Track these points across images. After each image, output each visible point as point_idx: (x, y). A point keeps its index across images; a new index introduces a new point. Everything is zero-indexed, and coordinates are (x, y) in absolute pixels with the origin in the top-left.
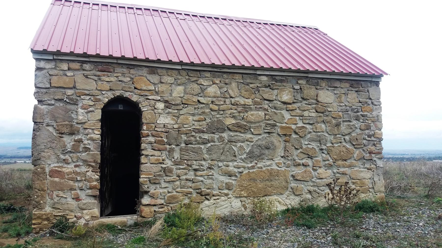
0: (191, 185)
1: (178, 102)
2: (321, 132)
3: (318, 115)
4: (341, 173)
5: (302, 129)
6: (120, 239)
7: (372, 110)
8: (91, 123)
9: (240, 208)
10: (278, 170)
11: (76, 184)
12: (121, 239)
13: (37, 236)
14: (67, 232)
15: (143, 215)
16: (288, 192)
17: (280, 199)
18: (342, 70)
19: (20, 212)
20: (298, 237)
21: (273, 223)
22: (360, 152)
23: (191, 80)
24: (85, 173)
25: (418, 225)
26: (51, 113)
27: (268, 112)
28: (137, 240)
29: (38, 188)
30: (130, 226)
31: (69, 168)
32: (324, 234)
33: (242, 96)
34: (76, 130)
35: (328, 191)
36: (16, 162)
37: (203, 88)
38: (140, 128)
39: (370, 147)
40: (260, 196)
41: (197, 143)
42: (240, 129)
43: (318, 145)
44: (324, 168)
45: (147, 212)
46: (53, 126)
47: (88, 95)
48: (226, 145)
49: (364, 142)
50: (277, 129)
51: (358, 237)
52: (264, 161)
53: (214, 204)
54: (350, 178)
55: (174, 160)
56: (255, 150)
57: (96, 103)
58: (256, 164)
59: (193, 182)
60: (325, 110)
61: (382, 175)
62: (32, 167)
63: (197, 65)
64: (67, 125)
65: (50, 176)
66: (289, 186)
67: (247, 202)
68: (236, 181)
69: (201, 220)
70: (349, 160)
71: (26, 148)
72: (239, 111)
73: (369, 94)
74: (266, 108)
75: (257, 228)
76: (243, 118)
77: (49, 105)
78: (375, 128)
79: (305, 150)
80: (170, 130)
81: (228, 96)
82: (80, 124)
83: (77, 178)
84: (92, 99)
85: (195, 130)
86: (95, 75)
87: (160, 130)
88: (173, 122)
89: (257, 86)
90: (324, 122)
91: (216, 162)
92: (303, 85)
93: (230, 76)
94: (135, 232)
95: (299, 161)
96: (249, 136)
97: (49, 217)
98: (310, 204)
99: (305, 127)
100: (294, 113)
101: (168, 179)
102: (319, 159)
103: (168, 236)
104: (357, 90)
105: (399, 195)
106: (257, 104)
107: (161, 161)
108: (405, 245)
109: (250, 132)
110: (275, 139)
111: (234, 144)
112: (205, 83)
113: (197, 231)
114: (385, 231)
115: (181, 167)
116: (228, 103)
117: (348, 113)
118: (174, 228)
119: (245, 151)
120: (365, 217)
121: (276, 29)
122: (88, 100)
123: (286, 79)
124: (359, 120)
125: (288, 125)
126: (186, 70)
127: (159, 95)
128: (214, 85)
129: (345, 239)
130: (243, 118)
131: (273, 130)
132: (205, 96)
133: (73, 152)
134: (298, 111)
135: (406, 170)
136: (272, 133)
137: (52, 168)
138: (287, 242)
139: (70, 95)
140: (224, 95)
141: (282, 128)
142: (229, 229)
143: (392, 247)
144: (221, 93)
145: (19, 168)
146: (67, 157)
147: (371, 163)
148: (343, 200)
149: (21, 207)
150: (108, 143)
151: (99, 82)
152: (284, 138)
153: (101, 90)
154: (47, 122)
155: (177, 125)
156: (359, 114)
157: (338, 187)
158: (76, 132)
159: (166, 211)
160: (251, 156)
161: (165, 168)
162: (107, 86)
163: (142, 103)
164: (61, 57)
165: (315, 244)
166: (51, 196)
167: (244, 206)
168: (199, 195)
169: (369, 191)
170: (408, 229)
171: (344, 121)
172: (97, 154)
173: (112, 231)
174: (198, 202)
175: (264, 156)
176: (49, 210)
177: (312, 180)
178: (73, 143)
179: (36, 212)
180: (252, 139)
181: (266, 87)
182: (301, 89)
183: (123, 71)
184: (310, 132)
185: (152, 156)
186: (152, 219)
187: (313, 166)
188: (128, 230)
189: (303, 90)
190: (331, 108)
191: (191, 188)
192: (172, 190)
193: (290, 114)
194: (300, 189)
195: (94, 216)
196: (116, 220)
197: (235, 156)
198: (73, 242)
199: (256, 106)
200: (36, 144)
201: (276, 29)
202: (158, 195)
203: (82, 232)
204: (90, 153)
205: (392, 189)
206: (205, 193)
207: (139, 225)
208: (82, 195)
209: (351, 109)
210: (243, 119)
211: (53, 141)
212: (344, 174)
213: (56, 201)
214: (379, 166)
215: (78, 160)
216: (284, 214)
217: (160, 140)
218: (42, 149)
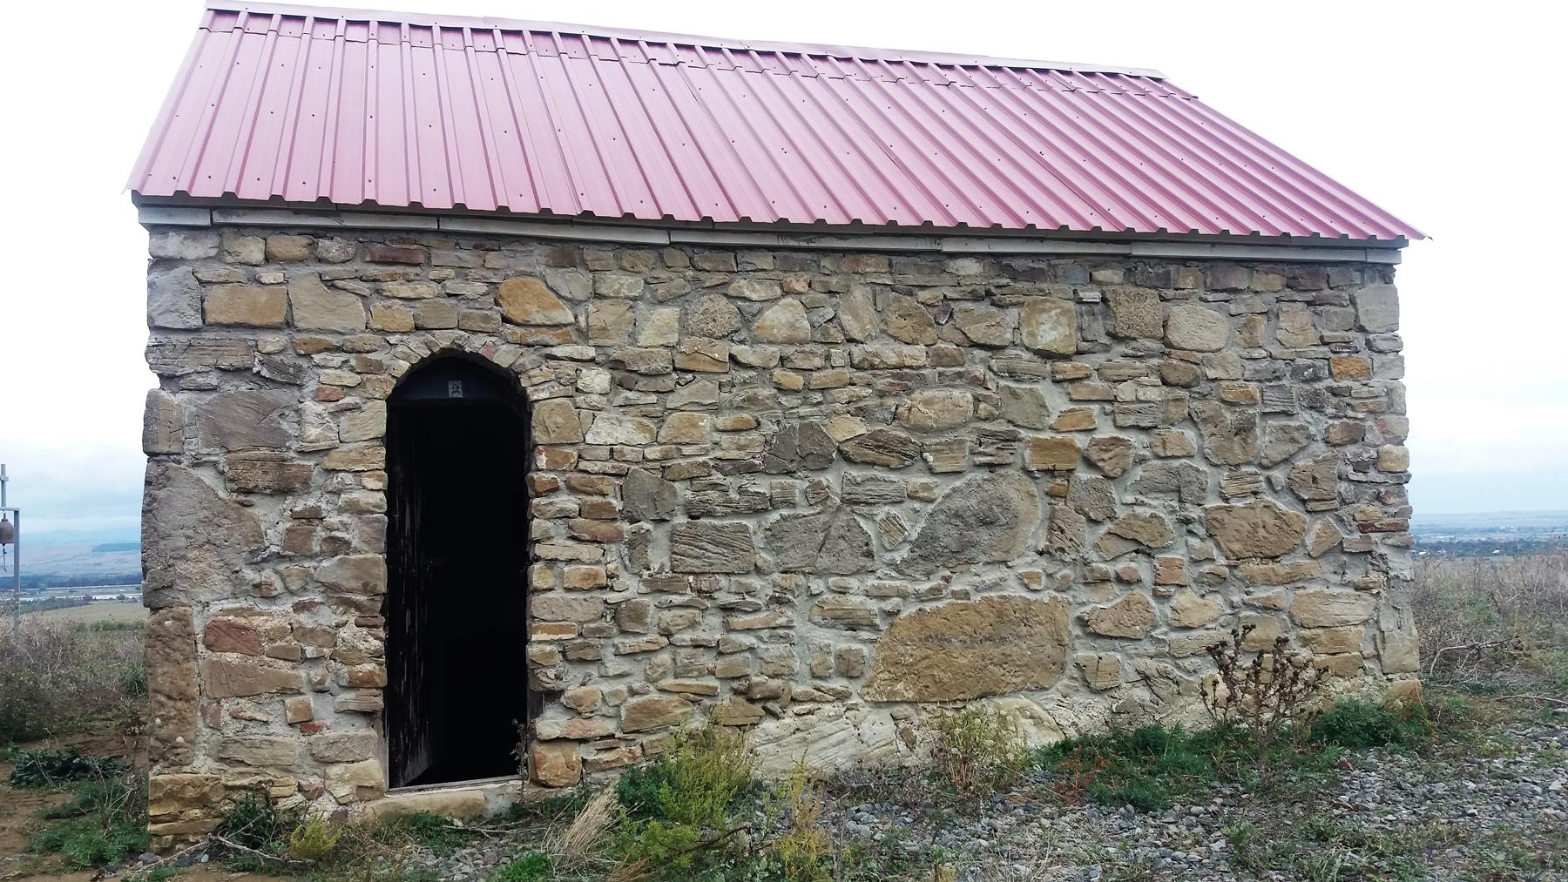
0: (711, 666)
1: (659, 365)
2: (1183, 457)
3: (1170, 396)
4: (1257, 604)
5: (1111, 448)
6: (461, 864)
7: (1368, 372)
8: (351, 451)
9: (891, 743)
13: (166, 863)
14: (271, 844)
15: (542, 775)
16: (1066, 681)
17: (1036, 707)
18: (1254, 227)
19: (106, 777)
20: (1104, 844)
21: (1014, 793)
23: (704, 282)
24: (333, 632)
25: (1546, 790)
26: (207, 419)
27: (988, 389)
28: (523, 867)
29: (167, 687)
30: (497, 818)
31: (274, 617)
32: (1199, 830)
33: (890, 336)
36: (90, 599)
37: (749, 310)
38: (526, 463)
39: (1363, 507)
40: (961, 696)
41: (729, 510)
42: (884, 457)
46: (215, 464)
47: (339, 349)
49: (1342, 490)
50: (1019, 451)
51: (1322, 837)
52: (973, 569)
53: (798, 729)
54: (1293, 622)
55: (651, 576)
56: (941, 531)
59: (721, 654)
60: (1197, 378)
61: (1409, 607)
62: (145, 615)
63: (726, 228)
64: (264, 460)
65: (208, 647)
66: (1067, 658)
67: (917, 722)
68: (877, 645)
69: (749, 792)
70: (1288, 557)
71: (125, 547)
72: (880, 391)
74: (977, 374)
75: (953, 814)
77: (200, 390)
78: (1381, 436)
79: (1124, 525)
80: (634, 467)
81: (840, 338)
83: (303, 651)
84: (353, 362)
85: (721, 465)
86: (361, 279)
87: (596, 469)
88: (642, 438)
89: (945, 296)
90: (1192, 418)
91: (801, 579)
92: (1113, 287)
93: (846, 264)
94: (515, 841)
95: (1102, 565)
96: (917, 479)
97: (205, 793)
98: (1146, 721)
99: (1123, 440)
100: (1080, 391)
101: (629, 643)
103: (632, 850)
104: (1312, 299)
105: (1475, 680)
106: (945, 361)
107: (604, 581)
108: (1497, 862)
110: (1013, 489)
111: (865, 509)
112: (754, 290)
113: (736, 831)
114: (1423, 813)
115: (677, 599)
116: (838, 362)
117: (1280, 383)
118: (654, 824)
120: (1350, 765)
121: (1009, 86)
122: (340, 367)
123: (1050, 265)
124: (1320, 410)
125: (1059, 436)
126: (685, 248)
127: (591, 342)
128: (789, 300)
129: (1274, 848)
130: (895, 414)
131: (1006, 457)
132: (756, 341)
133: (290, 559)
134: (1096, 382)
135: (1501, 586)
136: (1001, 465)
137: (213, 618)
138: (1065, 864)
139: (275, 354)
140: (826, 333)
141: (1039, 446)
142: (853, 819)
143: (1447, 871)
144: (813, 326)
145: (100, 620)
146: (268, 574)
147: (1370, 567)
148: (1267, 706)
149: (110, 759)
152: (1048, 484)
153: (383, 332)
154: (193, 453)
156: (1319, 386)
157: (1248, 656)
159: (626, 760)
160: (928, 552)
162: (404, 316)
163: (532, 373)
164: (238, 216)
165: (1165, 868)
167: (904, 734)
168: (741, 699)
170: (1507, 803)
171: (1265, 414)
172: (375, 562)
173: (430, 837)
174: (739, 727)
175: (973, 552)
176: (206, 768)
177: (1153, 634)
178: (288, 525)
179: (159, 775)
180: (931, 489)
181: (976, 298)
182: (1104, 300)
183: (460, 258)
184: (1142, 460)
185: (569, 561)
186: (575, 790)
188: (488, 833)
189: (1111, 304)
191: (714, 674)
193: (1069, 394)
194: (1108, 669)
195: (366, 784)
196: (444, 796)
197: (870, 555)
199: (940, 369)
200: (156, 530)
201: (1009, 86)
202: (594, 703)
203: (324, 842)
204: (350, 560)
205: (1449, 659)
206: (762, 692)
207: (527, 814)
208: (323, 709)
209: (1290, 368)
211: (216, 520)
212: (1269, 609)
213: (231, 735)
214: (1398, 577)
216: (1053, 762)
217: (596, 505)
218: (179, 548)
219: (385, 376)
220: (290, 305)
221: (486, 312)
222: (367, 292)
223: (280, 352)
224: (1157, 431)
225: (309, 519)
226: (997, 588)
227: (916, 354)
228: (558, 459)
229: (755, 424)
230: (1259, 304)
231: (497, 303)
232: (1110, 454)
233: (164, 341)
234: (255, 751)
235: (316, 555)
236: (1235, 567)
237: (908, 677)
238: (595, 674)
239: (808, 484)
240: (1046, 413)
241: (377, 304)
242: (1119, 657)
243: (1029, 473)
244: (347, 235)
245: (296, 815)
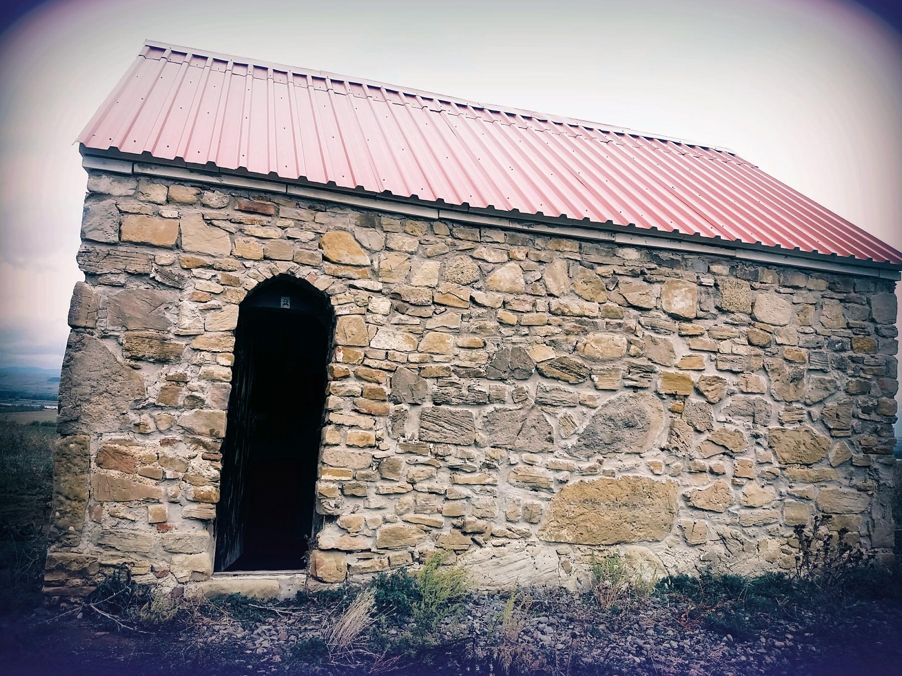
0: (439, 507)
1: (425, 298)
2: (758, 393)
3: (753, 353)
4: (796, 495)
5: (713, 383)
10: (653, 482)
11: (162, 488)
16: (672, 537)
21: (641, 615)
22: (843, 447)
23: (458, 246)
24: (186, 461)
26: (116, 306)
27: (637, 336)
30: (287, 602)
31: (149, 447)
34: (172, 352)
37: (486, 268)
39: (866, 436)
41: (461, 401)
43: (749, 426)
44: (758, 482)
46: (117, 337)
47: (210, 267)
48: (531, 412)
49: (854, 424)
50: (654, 379)
52: (619, 456)
54: (817, 508)
56: (599, 428)
57: (228, 290)
58: (601, 462)
59: (447, 499)
61: (890, 505)
63: (478, 212)
64: (151, 338)
65: (99, 465)
67: (573, 558)
68: (551, 502)
70: (817, 465)
72: (567, 331)
73: (871, 308)
74: (631, 326)
77: (113, 285)
78: (881, 391)
80: (401, 366)
81: (544, 293)
82: (184, 339)
83: (164, 473)
84: (219, 277)
86: (230, 221)
87: (375, 365)
88: (408, 347)
89: (614, 271)
91: (503, 453)
92: (723, 277)
93: (552, 244)
95: (702, 461)
96: (585, 392)
97: (85, 568)
100: (697, 344)
101: (386, 486)
106: (611, 315)
107: (373, 442)
109: (590, 382)
110: (648, 404)
111: (551, 409)
112: (490, 255)
115: (421, 459)
117: (821, 350)
119: (576, 428)
122: (210, 279)
123: (683, 258)
124: (844, 371)
126: (447, 222)
127: (380, 279)
128: (512, 264)
130: (575, 347)
132: (488, 289)
133: (162, 408)
134: (706, 338)
136: (641, 388)
137: (104, 445)
141: (667, 378)
146: (145, 417)
150: (246, 388)
152: (671, 403)
153: (241, 258)
154: (103, 329)
155: (419, 355)
156: (843, 354)
158: (172, 358)
161: (382, 459)
162: (256, 249)
163: (339, 296)
166: (97, 514)
167: (563, 565)
168: (457, 531)
169: (860, 543)
172: (220, 416)
174: (455, 551)
175: (618, 445)
176: (88, 550)
177: (730, 509)
178: (163, 385)
180: (595, 400)
181: (635, 275)
182: (716, 285)
184: (732, 394)
185: (352, 426)
190: (784, 337)
192: (393, 515)
193: (689, 345)
194: (700, 531)
197: (551, 440)
200: (70, 380)
208: (175, 515)
209: (827, 341)
210: (574, 350)
211: (113, 377)
212: (804, 498)
213: (108, 528)
215: (172, 427)
218: (85, 394)
219: (240, 289)
220: (180, 234)
221: (312, 252)
222: (233, 230)
223: (170, 265)
224: (743, 375)
225: (177, 382)
226: (633, 471)
227: (592, 308)
228: (351, 356)
229: (483, 345)
230: (812, 297)
231: (320, 247)
232: (712, 387)
233: (91, 249)
234: (124, 541)
235: (180, 407)
236: (784, 469)
237: (570, 526)
238: (362, 506)
239: (514, 389)
240: (673, 356)
241: (239, 239)
242: (707, 523)
243: (659, 394)
244: (224, 190)
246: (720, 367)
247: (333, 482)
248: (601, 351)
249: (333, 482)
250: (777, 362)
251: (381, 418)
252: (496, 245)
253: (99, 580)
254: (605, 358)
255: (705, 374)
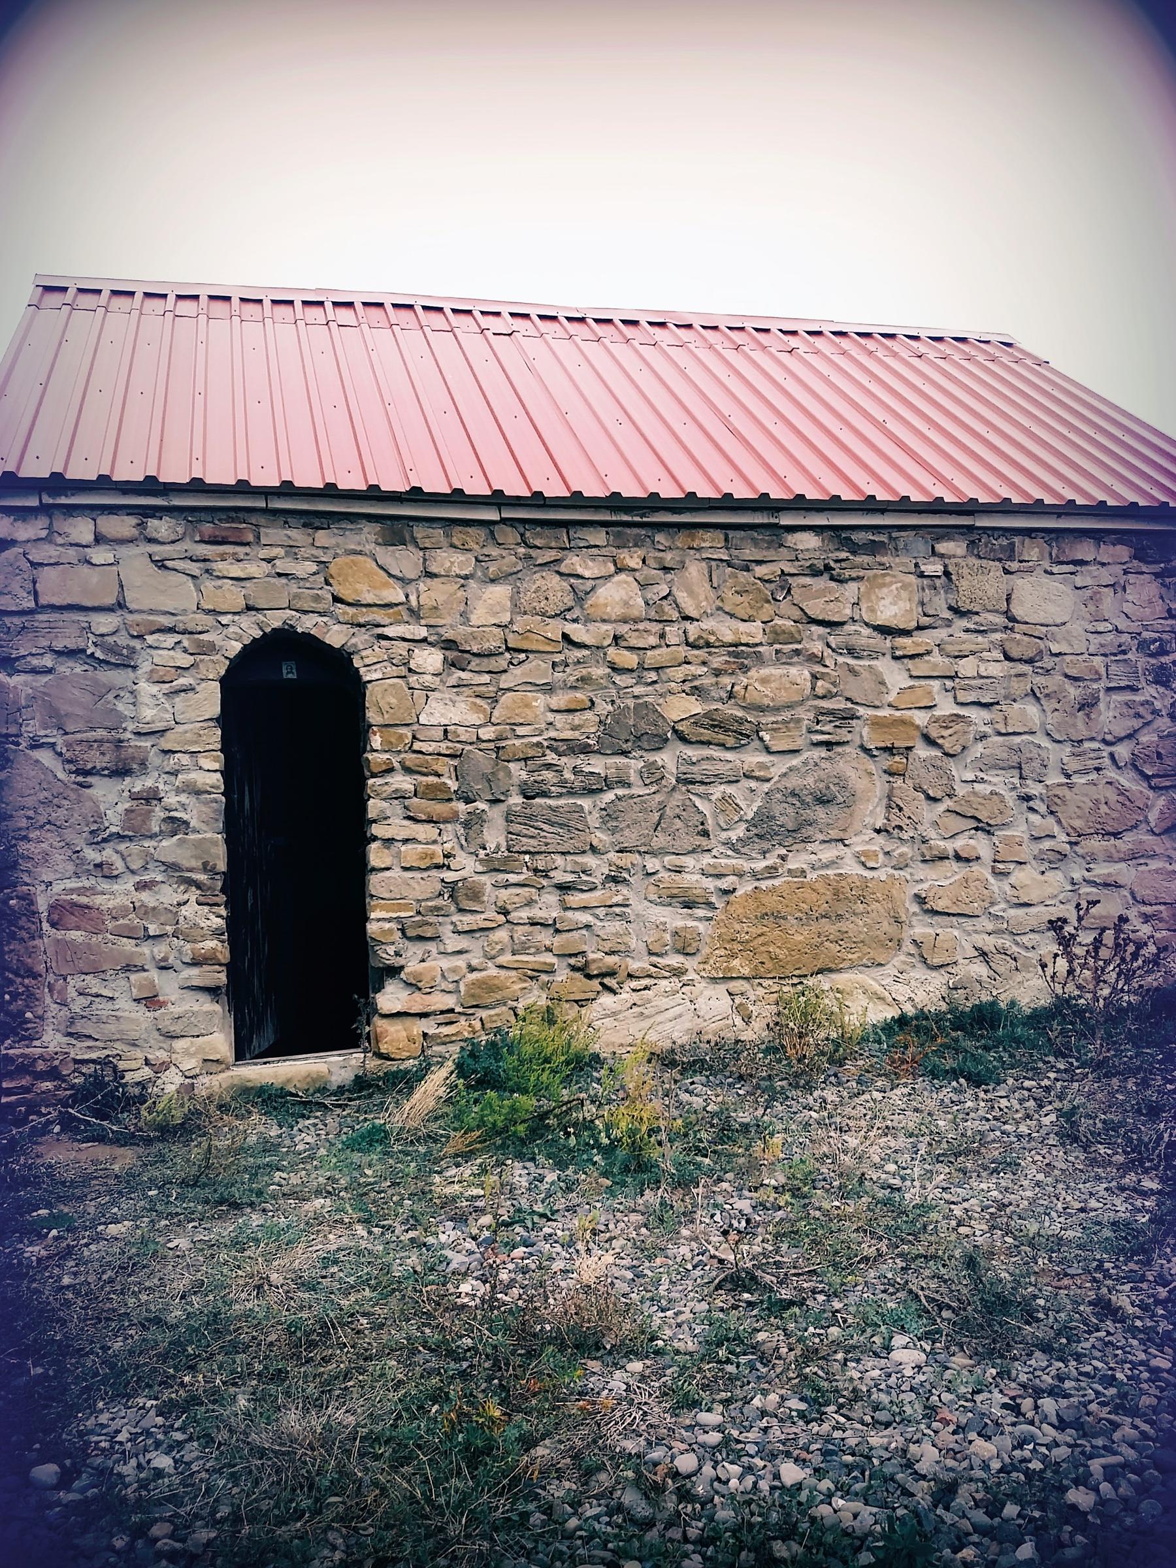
0: (548, 943)
1: (492, 644)
2: (1025, 733)
3: (1013, 672)
8: (186, 732)
11: (146, 949)
12: (306, 1135)
16: (903, 958)
18: (1101, 496)
23: (536, 559)
24: (174, 910)
26: (44, 700)
27: (826, 666)
28: (363, 1137)
34: (133, 758)
35: (1048, 946)
37: (582, 587)
40: (797, 972)
41: (564, 790)
45: (398, 1040)
46: (53, 745)
47: (171, 630)
50: (857, 729)
52: (810, 847)
54: (1134, 898)
55: (487, 855)
56: (777, 810)
57: (202, 661)
58: (783, 858)
59: (557, 931)
60: (1041, 652)
64: (100, 741)
67: (753, 998)
70: (1130, 833)
72: (715, 669)
74: (815, 651)
76: (731, 695)
81: (675, 615)
82: (147, 737)
83: (146, 929)
84: (186, 643)
85: (554, 745)
86: (191, 559)
87: (431, 750)
90: (1034, 694)
91: (636, 859)
93: (681, 540)
95: (941, 843)
96: (752, 758)
100: (919, 667)
102: (1015, 834)
106: (781, 638)
107: (440, 860)
111: (701, 789)
112: (587, 567)
115: (513, 878)
116: (672, 639)
117: (1126, 657)
123: (890, 538)
126: (517, 525)
127: (423, 622)
128: (622, 577)
132: (589, 620)
133: (130, 839)
134: (936, 658)
136: (838, 744)
140: (660, 611)
141: (877, 723)
142: (687, 1091)
144: (647, 604)
146: (108, 854)
148: (1105, 982)
151: (207, 584)
152: (886, 761)
155: (493, 728)
157: (1088, 932)
158: (135, 766)
163: (364, 653)
166: (59, 993)
167: (739, 1009)
168: (578, 975)
171: (1109, 689)
172: (215, 843)
174: (576, 1001)
175: (808, 831)
176: (55, 1043)
177: (991, 910)
178: (127, 805)
180: (768, 768)
181: (815, 572)
182: (947, 574)
184: (984, 737)
185: (406, 841)
187: (995, 861)
190: (1064, 642)
192: (482, 960)
193: (909, 670)
194: (946, 946)
197: (705, 834)
198: (140, 1150)
199: (778, 646)
202: (433, 979)
206: (599, 968)
208: (168, 986)
209: (1136, 642)
210: (730, 698)
211: (56, 801)
212: (1110, 885)
213: (78, 1010)
218: (20, 829)
223: (114, 633)
224: (998, 707)
227: (753, 632)
228: (393, 740)
229: (589, 704)
230: (1105, 575)
231: (327, 583)
232: (950, 731)
234: (102, 1026)
235: (156, 835)
236: (1076, 843)
238: (434, 951)
239: (643, 764)
242: (956, 933)
243: (866, 751)
245: (144, 1088)
246: (960, 699)
247: (389, 920)
248: (771, 695)
249: (389, 920)
250: (1054, 682)
251: (449, 825)
252: (595, 551)
253: (76, 1081)
254: (778, 704)
255: (937, 713)
